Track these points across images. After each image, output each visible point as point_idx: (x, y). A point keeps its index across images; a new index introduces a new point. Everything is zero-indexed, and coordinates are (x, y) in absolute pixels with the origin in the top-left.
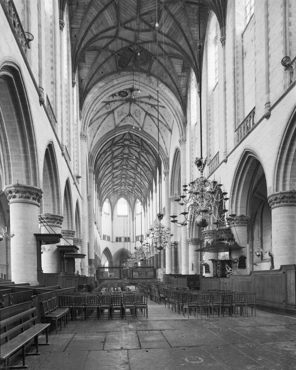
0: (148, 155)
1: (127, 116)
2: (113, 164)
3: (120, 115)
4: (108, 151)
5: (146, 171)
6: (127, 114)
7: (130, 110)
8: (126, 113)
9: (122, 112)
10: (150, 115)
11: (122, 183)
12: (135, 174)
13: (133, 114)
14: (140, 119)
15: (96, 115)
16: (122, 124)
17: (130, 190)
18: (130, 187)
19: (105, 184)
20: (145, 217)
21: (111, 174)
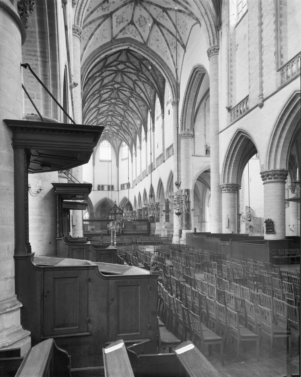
0: (146, 85)
1: (129, 24)
2: (100, 96)
3: (120, 23)
4: (97, 76)
5: (140, 106)
6: (129, 22)
7: (133, 15)
8: (127, 20)
9: (123, 18)
10: (158, 24)
11: (107, 122)
12: (125, 111)
13: (136, 22)
14: (144, 31)
15: (88, 16)
16: (121, 36)
17: (116, 131)
18: (116, 127)
19: (89, 120)
20: (132, 162)
21: (97, 109)
